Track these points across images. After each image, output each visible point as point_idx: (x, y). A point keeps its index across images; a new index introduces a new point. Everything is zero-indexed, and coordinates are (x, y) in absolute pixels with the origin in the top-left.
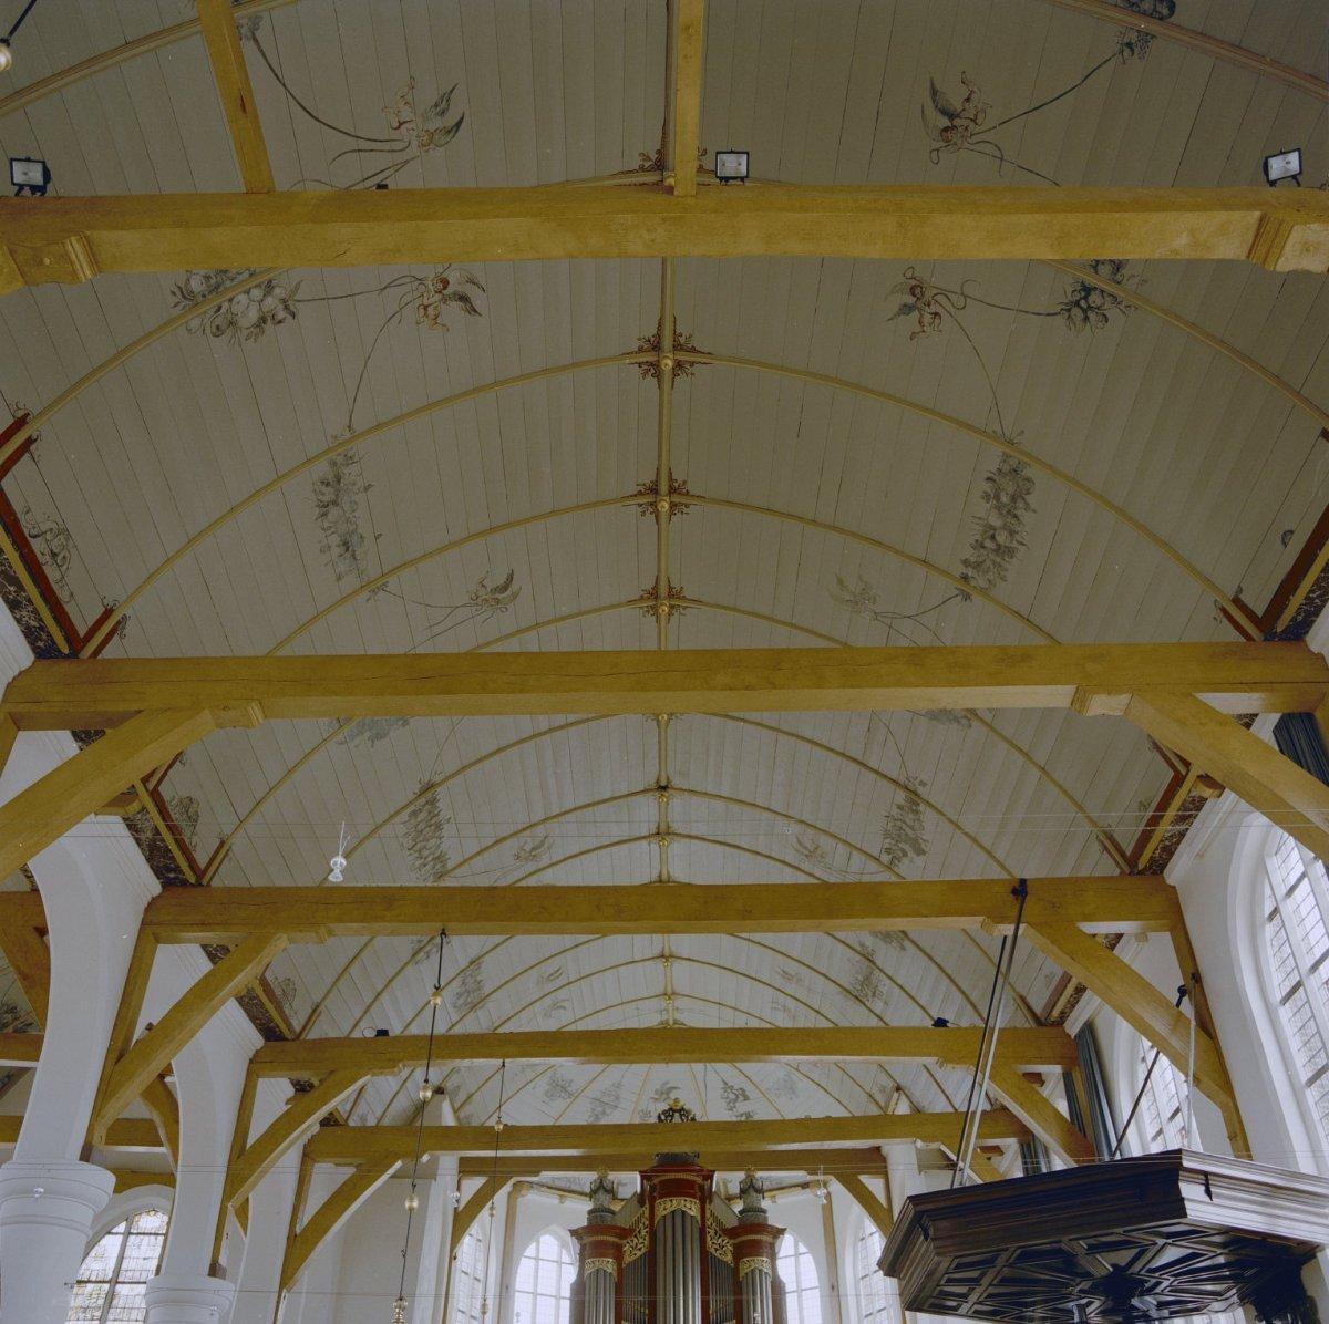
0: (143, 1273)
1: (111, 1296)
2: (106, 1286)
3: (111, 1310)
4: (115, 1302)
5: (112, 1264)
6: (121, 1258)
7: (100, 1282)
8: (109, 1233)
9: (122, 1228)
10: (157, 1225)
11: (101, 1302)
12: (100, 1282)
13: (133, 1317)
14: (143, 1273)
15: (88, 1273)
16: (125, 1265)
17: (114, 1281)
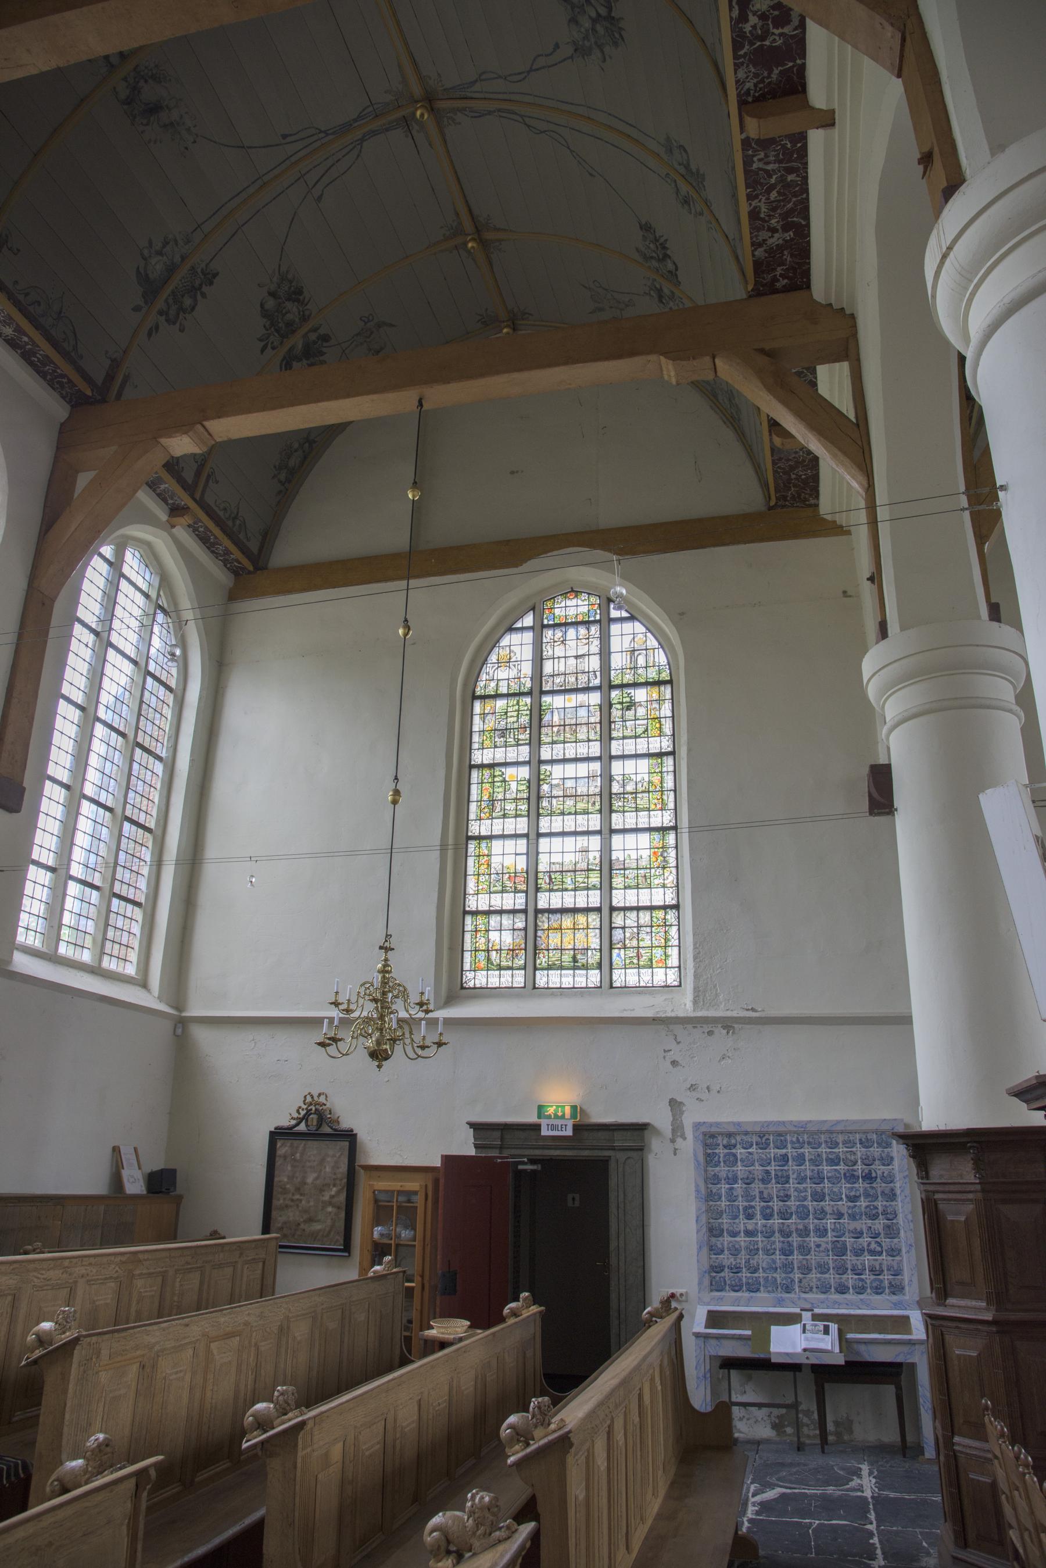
0: (580, 676)
1: (537, 714)
3: (544, 730)
4: (546, 719)
5: (527, 669)
7: (514, 695)
8: (511, 629)
9: (528, 620)
10: (585, 609)
11: (524, 720)
12: (514, 695)
13: (582, 736)
14: (580, 676)
15: (493, 684)
16: (548, 668)
17: (537, 690)
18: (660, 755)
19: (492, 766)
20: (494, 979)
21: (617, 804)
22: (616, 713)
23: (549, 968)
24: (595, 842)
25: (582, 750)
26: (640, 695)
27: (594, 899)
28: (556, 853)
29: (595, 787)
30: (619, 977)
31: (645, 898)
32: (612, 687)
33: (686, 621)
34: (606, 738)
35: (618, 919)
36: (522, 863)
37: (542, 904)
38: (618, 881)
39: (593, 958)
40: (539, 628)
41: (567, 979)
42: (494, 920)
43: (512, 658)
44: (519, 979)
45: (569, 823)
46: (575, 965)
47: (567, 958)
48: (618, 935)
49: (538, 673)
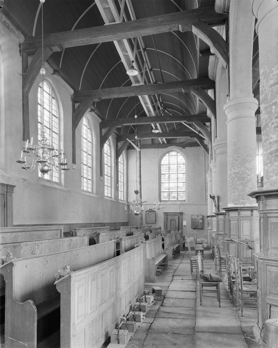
1: (169, 168)
2: (168, 166)
5: (168, 162)
6: (169, 161)
9: (167, 155)
11: (168, 168)
17: (169, 164)
18: (184, 173)
19: (164, 174)
20: (165, 199)
21: (179, 179)
22: (179, 168)
23: (171, 198)
24: (176, 184)
25: (175, 172)
26: (181, 165)
27: (176, 190)
28: (172, 185)
29: (176, 177)
30: (179, 199)
31: (181, 190)
32: (178, 164)
33: (187, 157)
34: (177, 171)
35: (179, 193)
36: (168, 186)
37: (170, 191)
38: (179, 188)
39: (176, 197)
40: (169, 156)
41: (173, 199)
42: (165, 193)
43: (165, 160)
44: (168, 199)
45: (173, 181)
46: (174, 198)
47: (173, 197)
48: (179, 195)
49: (169, 163)
